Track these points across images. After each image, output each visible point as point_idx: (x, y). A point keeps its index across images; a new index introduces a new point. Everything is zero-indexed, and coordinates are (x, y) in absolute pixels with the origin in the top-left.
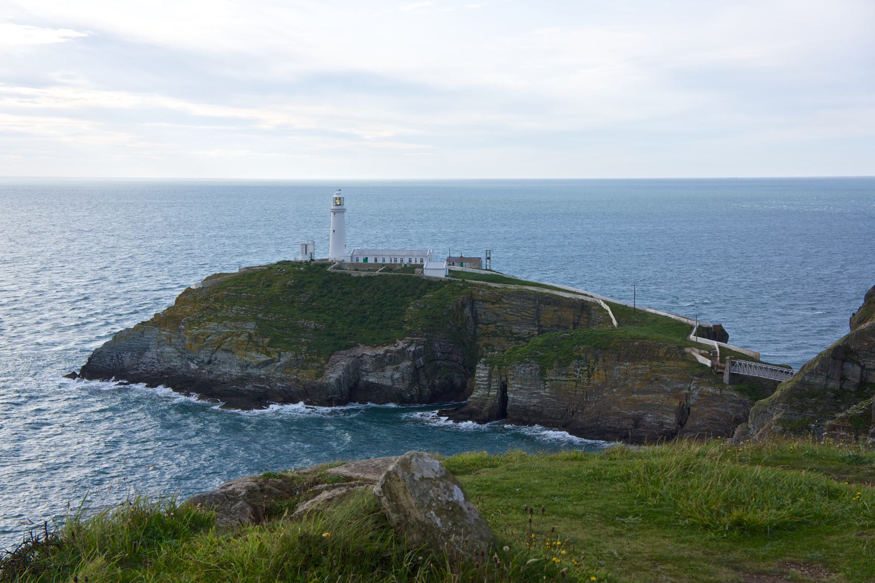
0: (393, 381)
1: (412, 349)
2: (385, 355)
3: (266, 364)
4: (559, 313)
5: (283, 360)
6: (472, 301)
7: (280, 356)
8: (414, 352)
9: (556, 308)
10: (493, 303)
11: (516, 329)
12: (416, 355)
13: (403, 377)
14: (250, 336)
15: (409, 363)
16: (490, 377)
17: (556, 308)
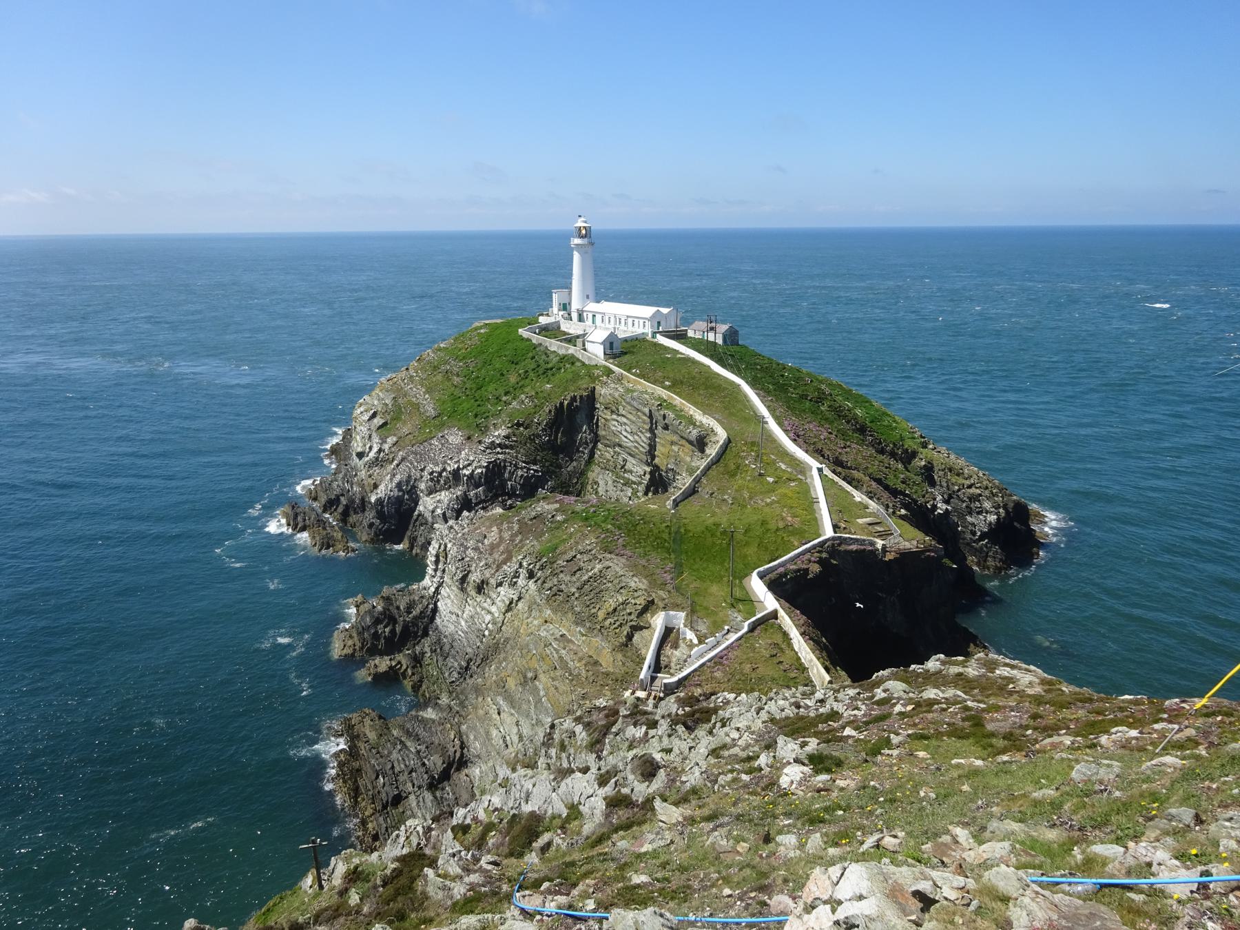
0: (433, 517)
1: (467, 472)
2: (440, 474)
3: (360, 455)
4: (675, 448)
5: (372, 454)
6: (590, 400)
7: (371, 448)
8: (471, 476)
9: (675, 438)
10: (612, 412)
11: (632, 463)
12: (473, 481)
13: (444, 514)
14: (374, 415)
15: (459, 491)
16: (437, 556)
17: (675, 438)
